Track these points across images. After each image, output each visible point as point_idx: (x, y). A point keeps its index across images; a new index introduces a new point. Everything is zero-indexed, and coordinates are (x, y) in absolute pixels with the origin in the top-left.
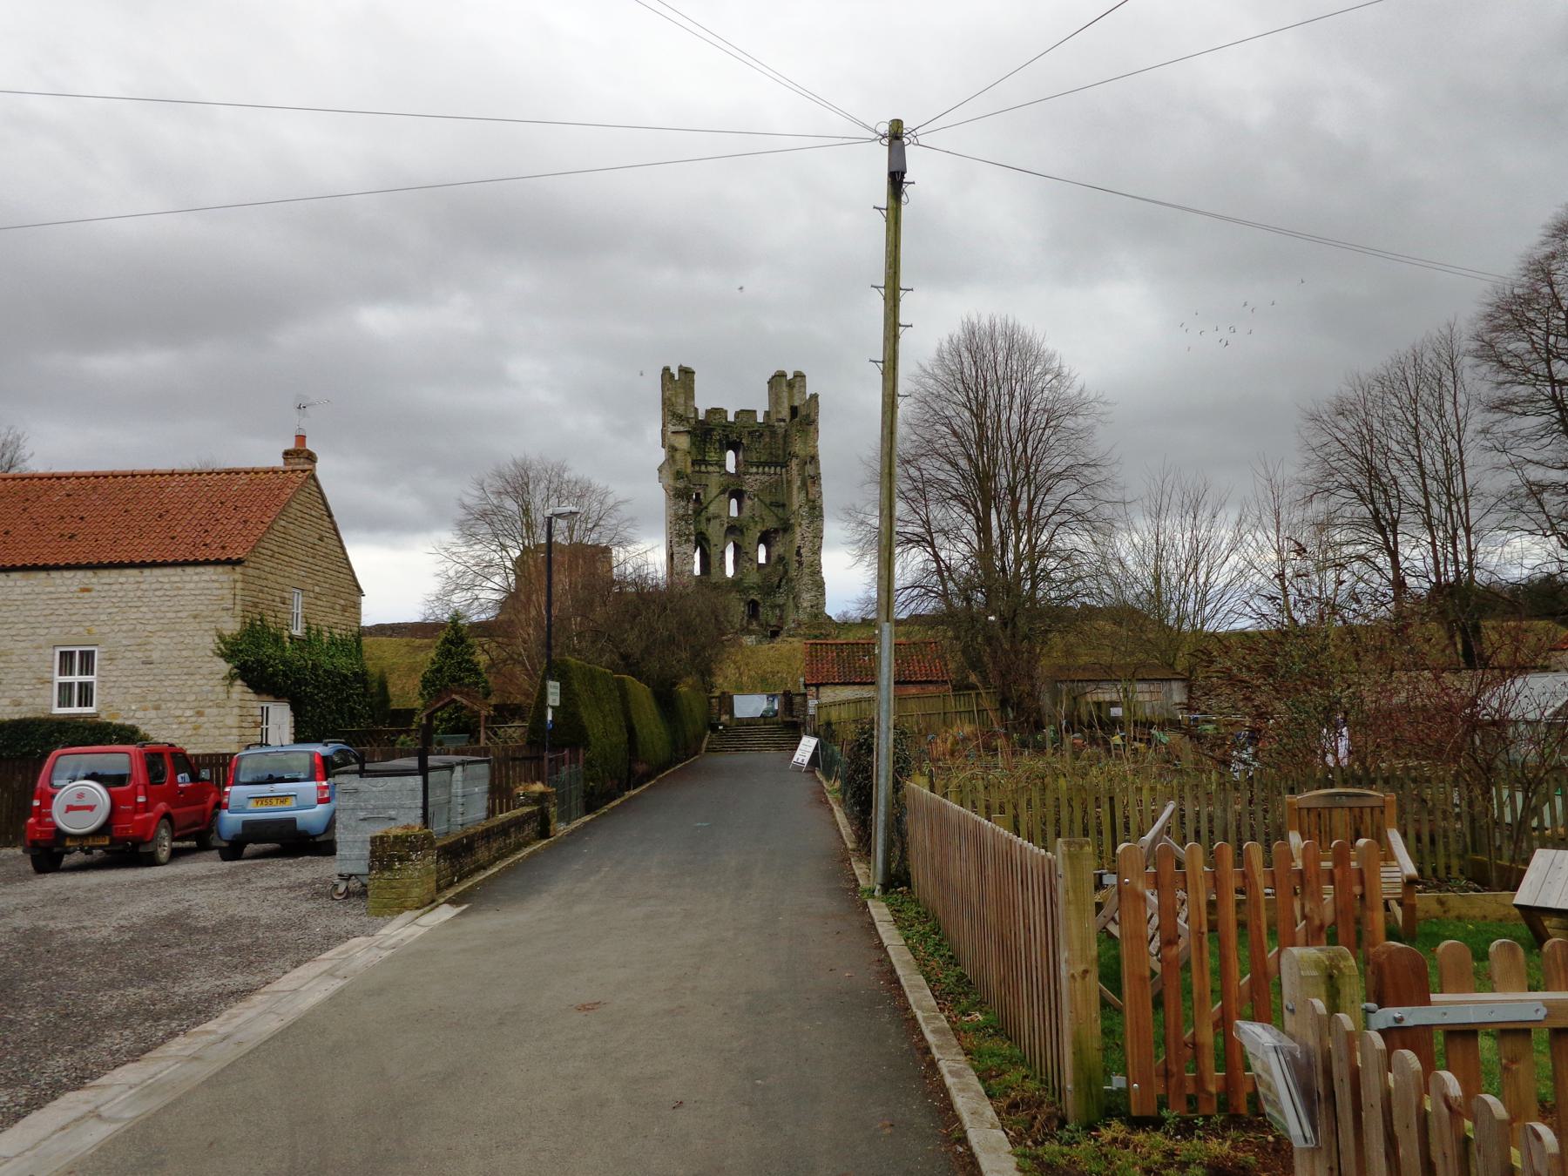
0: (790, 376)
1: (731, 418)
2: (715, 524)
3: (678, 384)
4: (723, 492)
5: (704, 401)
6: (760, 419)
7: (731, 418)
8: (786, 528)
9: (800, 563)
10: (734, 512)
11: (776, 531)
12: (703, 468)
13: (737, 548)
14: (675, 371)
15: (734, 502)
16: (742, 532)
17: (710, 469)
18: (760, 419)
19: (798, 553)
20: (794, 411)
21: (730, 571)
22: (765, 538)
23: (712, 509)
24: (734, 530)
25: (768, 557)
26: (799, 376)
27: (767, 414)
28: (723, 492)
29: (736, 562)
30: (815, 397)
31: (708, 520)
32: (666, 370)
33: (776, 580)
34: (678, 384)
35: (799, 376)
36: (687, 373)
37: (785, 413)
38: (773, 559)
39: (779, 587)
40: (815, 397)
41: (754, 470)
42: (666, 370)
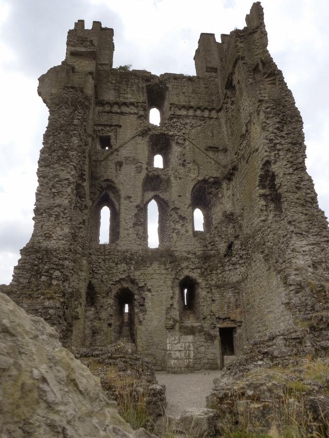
2: (129, 170)
10: (158, 161)
11: (217, 183)
12: (116, 109)
13: (163, 207)
16: (168, 181)
17: (125, 109)
21: (154, 241)
22: (202, 196)
23: (124, 153)
29: (162, 230)
31: (120, 164)
32: (81, 23)
33: (222, 247)
38: (217, 216)
42: (81, 23)
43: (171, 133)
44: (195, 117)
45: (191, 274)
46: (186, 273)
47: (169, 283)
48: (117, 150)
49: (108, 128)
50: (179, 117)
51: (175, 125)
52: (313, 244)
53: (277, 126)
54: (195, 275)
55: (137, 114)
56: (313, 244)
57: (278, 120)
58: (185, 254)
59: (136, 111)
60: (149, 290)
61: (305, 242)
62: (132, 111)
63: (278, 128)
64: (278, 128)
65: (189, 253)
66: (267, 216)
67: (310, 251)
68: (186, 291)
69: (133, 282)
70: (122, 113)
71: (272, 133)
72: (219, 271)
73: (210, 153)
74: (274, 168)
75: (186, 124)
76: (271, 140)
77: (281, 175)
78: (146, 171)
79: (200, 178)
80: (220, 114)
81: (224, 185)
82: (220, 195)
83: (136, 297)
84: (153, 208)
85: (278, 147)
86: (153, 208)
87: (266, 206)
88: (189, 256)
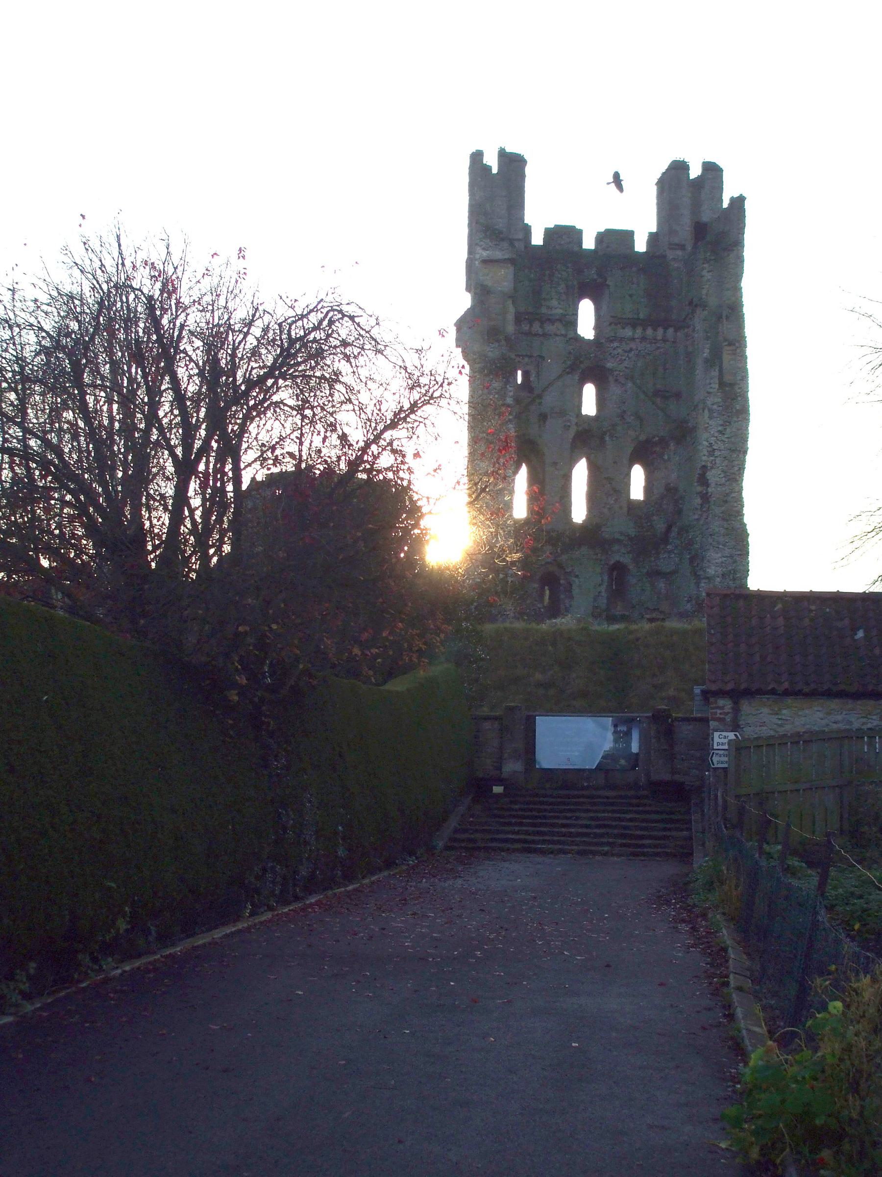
0: (695, 172)
1: (589, 243)
3: (497, 188)
4: (571, 369)
5: (542, 213)
6: (641, 245)
7: (589, 243)
8: (683, 433)
9: (705, 498)
12: (536, 327)
14: (492, 161)
15: (589, 392)
17: (550, 328)
18: (641, 245)
19: (703, 481)
20: (700, 230)
24: (587, 438)
25: (648, 489)
26: (713, 172)
27: (653, 239)
28: (571, 369)
30: (738, 203)
31: (543, 417)
32: (477, 157)
34: (497, 188)
35: (713, 172)
36: (513, 165)
37: (685, 233)
39: (665, 539)
40: (738, 203)
41: (628, 332)
42: (477, 157)
43: (609, 365)
44: (643, 339)
45: (622, 560)
46: (616, 558)
47: (598, 570)
48: (540, 396)
49: (526, 359)
50: (621, 340)
51: (616, 352)
52: (726, 557)
53: (720, 428)
54: (626, 560)
55: (565, 336)
56: (726, 557)
57: (721, 422)
58: (617, 536)
59: (563, 332)
60: (577, 576)
61: (719, 555)
62: (558, 333)
63: (720, 432)
64: (720, 432)
65: (621, 533)
66: (701, 515)
67: (722, 562)
68: (615, 573)
69: (560, 566)
70: (545, 335)
71: (713, 436)
72: (653, 559)
73: (658, 400)
74: (709, 475)
75: (631, 350)
76: (711, 444)
77: (713, 485)
78: (575, 427)
79: (643, 437)
80: (678, 334)
81: (672, 446)
82: (666, 457)
83: (562, 582)
84: (580, 473)
85: (717, 453)
86: (580, 473)
87: (702, 505)
88: (622, 538)
